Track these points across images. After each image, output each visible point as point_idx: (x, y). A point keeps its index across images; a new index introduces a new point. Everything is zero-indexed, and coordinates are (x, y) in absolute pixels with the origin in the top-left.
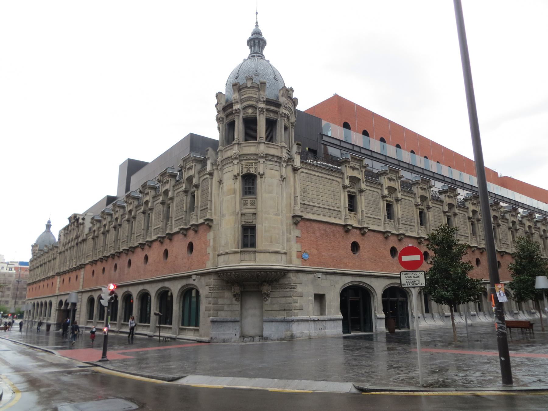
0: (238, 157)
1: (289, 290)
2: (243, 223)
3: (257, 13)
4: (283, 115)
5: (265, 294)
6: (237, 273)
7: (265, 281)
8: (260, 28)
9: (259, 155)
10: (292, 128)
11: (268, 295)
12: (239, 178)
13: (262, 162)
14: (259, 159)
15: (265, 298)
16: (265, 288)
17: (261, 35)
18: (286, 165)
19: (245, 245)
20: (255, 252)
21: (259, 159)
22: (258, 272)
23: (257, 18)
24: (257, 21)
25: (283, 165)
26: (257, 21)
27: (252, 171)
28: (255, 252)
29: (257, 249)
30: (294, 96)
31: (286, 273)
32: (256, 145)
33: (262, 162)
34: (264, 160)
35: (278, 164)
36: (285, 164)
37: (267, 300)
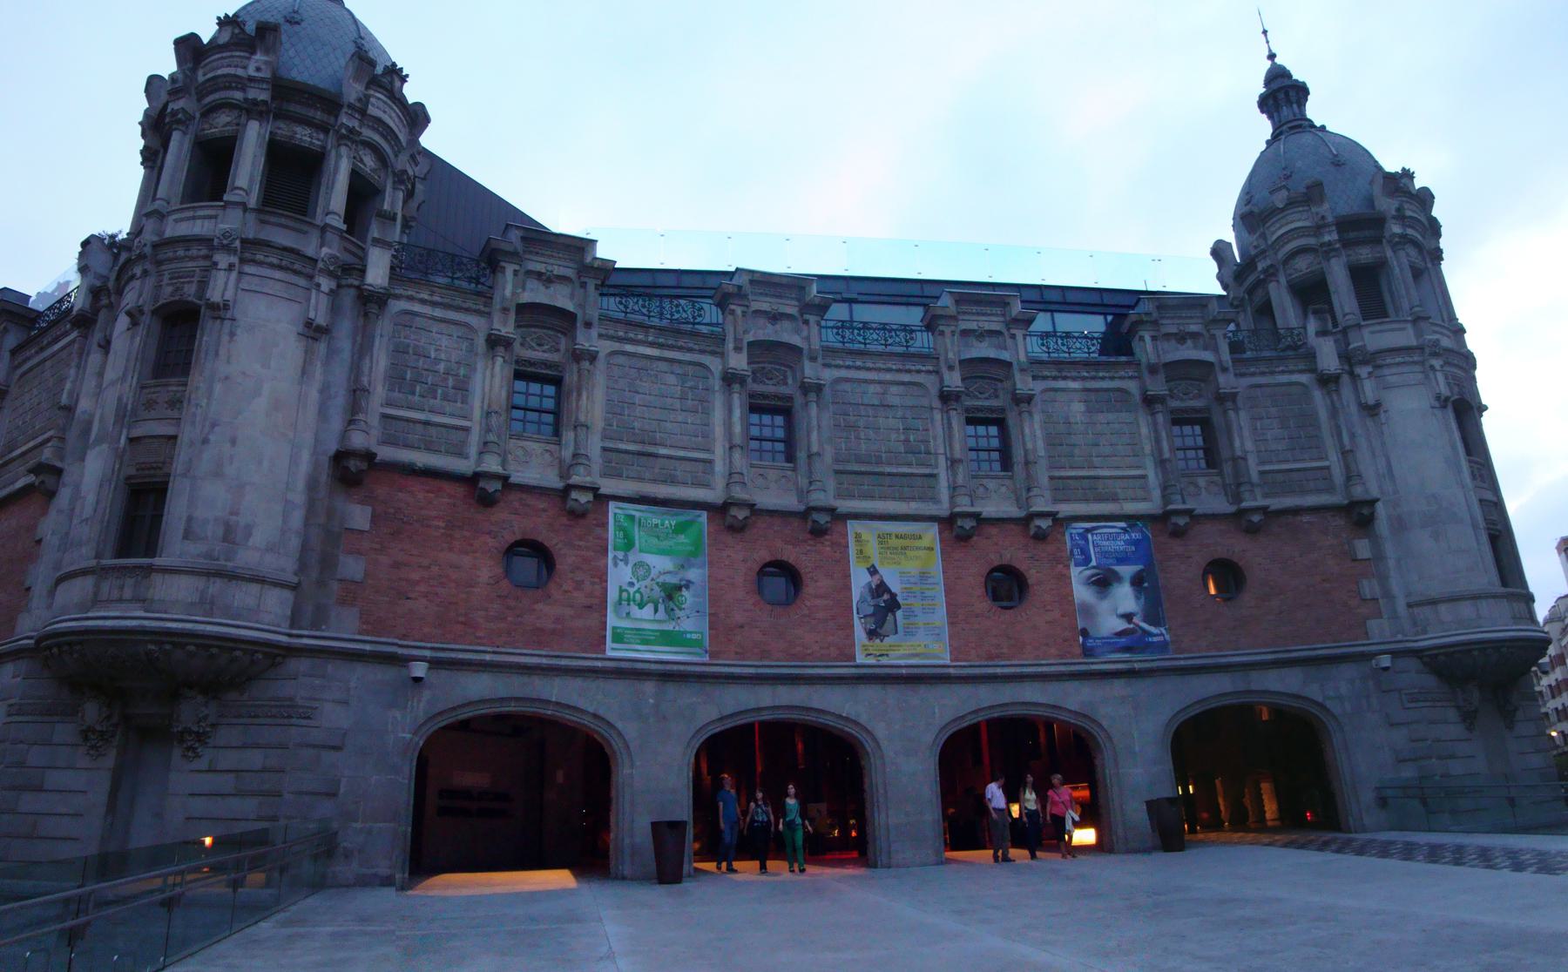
0: (148, 250)
1: (269, 721)
2: (132, 471)
4: (343, 131)
5: (190, 732)
6: (78, 647)
9: (216, 242)
10: (394, 189)
11: (201, 737)
12: (146, 319)
13: (223, 264)
14: (218, 257)
15: (188, 749)
16: (189, 712)
18: (333, 285)
19: (124, 549)
21: (218, 257)
22: (151, 642)
25: (318, 285)
27: (190, 290)
28: (150, 570)
29: (157, 561)
30: (411, 93)
31: (279, 659)
32: (220, 212)
33: (223, 264)
34: (234, 259)
35: (302, 282)
36: (326, 284)
37: (198, 756)
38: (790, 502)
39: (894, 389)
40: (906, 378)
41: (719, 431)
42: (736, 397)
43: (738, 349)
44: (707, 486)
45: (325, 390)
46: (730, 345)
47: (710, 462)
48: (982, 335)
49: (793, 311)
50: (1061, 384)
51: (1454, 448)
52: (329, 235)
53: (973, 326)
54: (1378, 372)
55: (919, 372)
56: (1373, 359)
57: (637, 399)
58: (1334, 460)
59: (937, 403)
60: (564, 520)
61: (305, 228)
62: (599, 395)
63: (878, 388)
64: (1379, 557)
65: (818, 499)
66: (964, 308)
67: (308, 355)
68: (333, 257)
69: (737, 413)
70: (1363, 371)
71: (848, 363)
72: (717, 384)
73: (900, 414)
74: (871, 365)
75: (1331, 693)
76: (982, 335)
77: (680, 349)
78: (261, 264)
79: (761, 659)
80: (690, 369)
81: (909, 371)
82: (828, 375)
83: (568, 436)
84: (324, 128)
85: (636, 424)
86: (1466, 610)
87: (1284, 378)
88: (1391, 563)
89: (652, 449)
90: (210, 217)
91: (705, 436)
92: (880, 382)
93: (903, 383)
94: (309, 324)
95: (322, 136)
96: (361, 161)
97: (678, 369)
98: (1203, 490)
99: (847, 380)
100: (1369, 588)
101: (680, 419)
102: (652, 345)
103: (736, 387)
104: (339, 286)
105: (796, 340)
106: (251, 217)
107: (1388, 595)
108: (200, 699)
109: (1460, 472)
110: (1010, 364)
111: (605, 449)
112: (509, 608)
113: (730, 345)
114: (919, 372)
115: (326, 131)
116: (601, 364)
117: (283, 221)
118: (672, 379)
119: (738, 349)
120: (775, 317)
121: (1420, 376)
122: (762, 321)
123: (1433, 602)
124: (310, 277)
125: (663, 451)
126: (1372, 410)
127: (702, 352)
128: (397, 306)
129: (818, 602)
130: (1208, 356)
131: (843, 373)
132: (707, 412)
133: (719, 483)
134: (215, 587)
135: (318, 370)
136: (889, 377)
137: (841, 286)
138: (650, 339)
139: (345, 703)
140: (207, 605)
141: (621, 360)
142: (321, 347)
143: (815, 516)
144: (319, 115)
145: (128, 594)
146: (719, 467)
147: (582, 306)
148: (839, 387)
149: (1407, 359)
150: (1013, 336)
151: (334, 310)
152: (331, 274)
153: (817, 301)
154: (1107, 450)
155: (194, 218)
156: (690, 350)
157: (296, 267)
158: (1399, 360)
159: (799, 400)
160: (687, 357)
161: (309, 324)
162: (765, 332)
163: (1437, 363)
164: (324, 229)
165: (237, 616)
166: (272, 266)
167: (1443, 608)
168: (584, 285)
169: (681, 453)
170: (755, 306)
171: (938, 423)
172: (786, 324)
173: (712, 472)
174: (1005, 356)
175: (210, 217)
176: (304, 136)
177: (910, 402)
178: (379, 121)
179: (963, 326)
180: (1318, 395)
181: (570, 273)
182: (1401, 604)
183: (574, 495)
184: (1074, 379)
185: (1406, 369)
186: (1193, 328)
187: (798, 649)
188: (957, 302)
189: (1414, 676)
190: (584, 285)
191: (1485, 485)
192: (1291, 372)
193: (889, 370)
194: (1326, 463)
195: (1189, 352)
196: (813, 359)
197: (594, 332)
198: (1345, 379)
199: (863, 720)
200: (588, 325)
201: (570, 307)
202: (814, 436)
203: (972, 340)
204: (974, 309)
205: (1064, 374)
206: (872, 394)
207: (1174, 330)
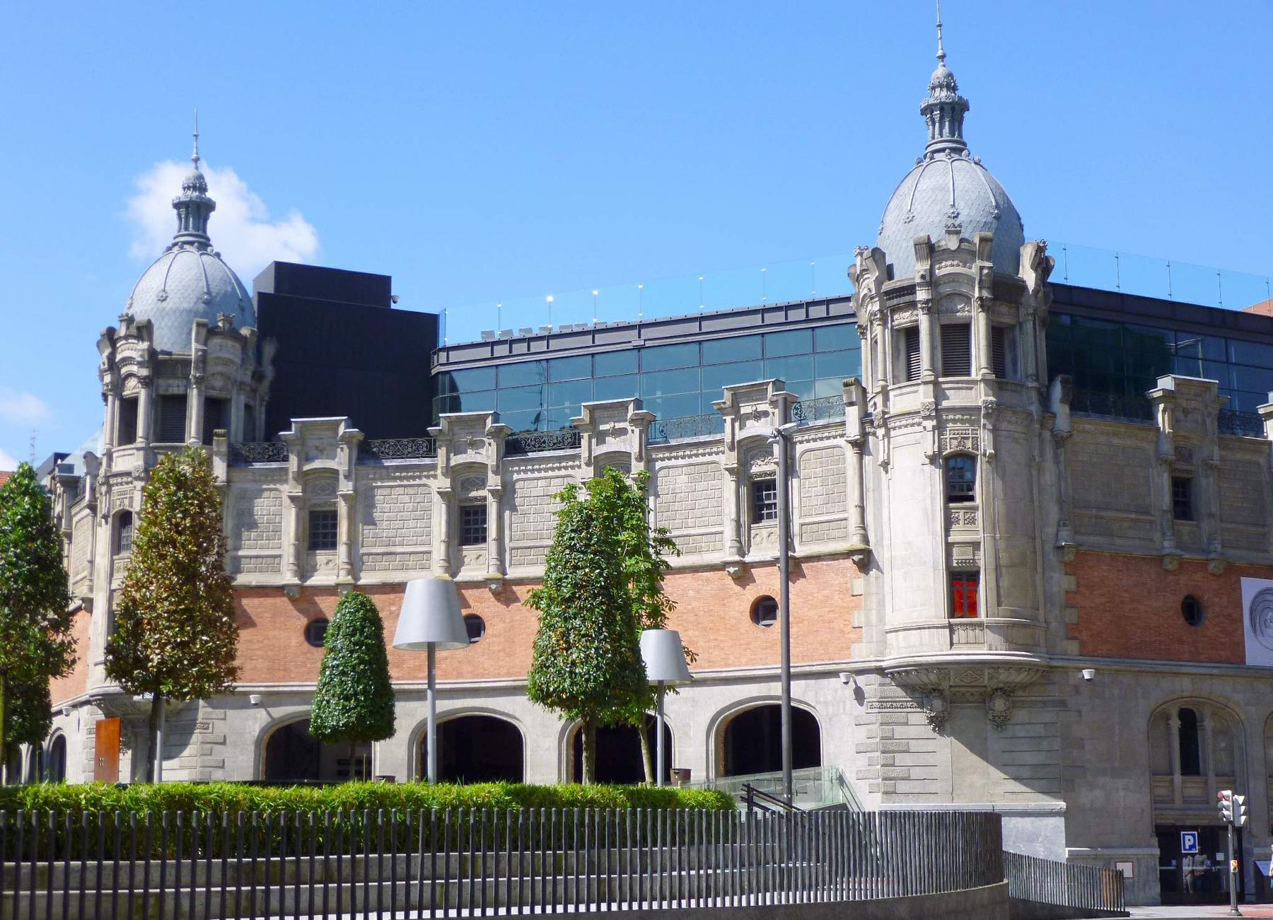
12: (110, 520)
50: (673, 462)
79: (457, 678)
90: (131, 455)
92: (545, 478)
97: (411, 491)
100: (857, 618)
109: (933, 520)
112: (309, 659)
118: (406, 498)
125: (399, 549)
128: (236, 486)
129: (495, 639)
136: (550, 473)
154: (698, 512)
155: (124, 455)
158: (904, 422)
175: (131, 455)
185: (910, 429)
187: (482, 670)
194: (845, 515)
199: (517, 715)
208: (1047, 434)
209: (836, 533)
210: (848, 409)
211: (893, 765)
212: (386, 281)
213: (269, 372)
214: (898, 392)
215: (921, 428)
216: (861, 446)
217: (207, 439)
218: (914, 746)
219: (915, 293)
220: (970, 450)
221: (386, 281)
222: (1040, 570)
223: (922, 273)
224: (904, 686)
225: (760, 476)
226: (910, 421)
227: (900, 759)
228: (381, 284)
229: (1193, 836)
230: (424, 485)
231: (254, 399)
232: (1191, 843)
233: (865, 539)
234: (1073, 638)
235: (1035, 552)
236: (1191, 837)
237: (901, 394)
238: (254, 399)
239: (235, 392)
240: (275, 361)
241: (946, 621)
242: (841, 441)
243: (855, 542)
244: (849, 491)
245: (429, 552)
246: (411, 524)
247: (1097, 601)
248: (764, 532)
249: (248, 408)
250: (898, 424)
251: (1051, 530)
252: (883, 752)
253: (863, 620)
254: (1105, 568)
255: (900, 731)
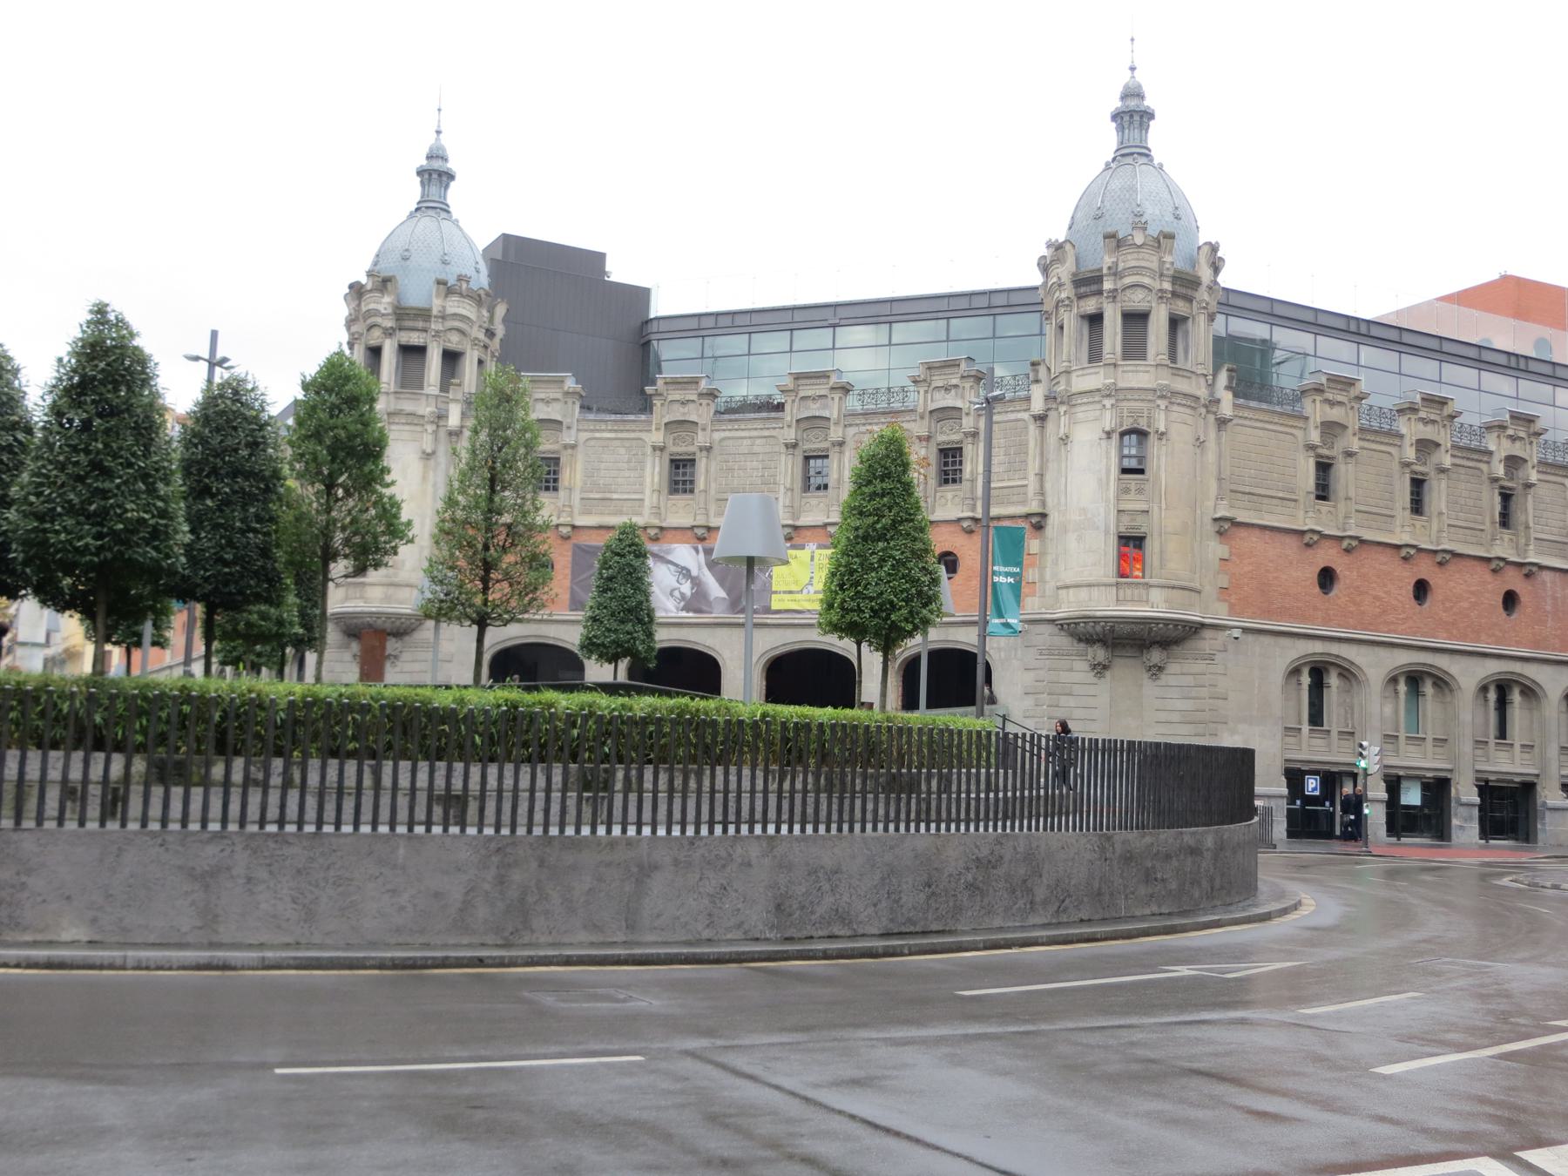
3: (439, 110)
7: (389, 634)
8: (445, 140)
11: (396, 657)
17: (445, 159)
18: (434, 427)
20: (363, 584)
23: (439, 121)
24: (439, 126)
26: (439, 126)
28: (363, 584)
35: (419, 428)
36: (430, 428)
38: (687, 521)
39: (758, 441)
40: (766, 433)
41: (648, 480)
42: (657, 459)
43: (657, 429)
44: (640, 514)
45: (435, 485)
46: (654, 427)
47: (642, 500)
48: (814, 399)
49: (694, 397)
51: (1108, 471)
52: (430, 399)
53: (809, 393)
54: (1074, 410)
55: (775, 428)
56: (1069, 399)
57: (603, 466)
58: (1032, 483)
59: (783, 449)
60: (559, 542)
61: (418, 397)
62: (579, 466)
63: (749, 442)
64: (1043, 553)
65: (701, 521)
66: (801, 382)
67: (425, 467)
68: (434, 412)
69: (657, 469)
70: (1063, 409)
71: (730, 427)
72: (649, 450)
73: (761, 457)
74: (743, 427)
75: (995, 645)
76: (814, 399)
77: (628, 431)
78: (397, 423)
80: (634, 443)
81: (768, 429)
82: (717, 436)
83: (562, 493)
84: (425, 330)
85: (601, 482)
86: (1084, 593)
87: (1012, 416)
88: (1049, 558)
89: (608, 495)
91: (641, 484)
92: (750, 438)
93: (765, 437)
94: (424, 452)
95: (424, 334)
96: (449, 341)
97: (627, 444)
98: (949, 503)
99: (729, 438)
101: (627, 475)
102: (610, 431)
103: (658, 453)
104: (438, 426)
105: (693, 418)
106: (392, 397)
107: (1042, 580)
108: (394, 640)
109: (1108, 489)
110: (828, 419)
111: (582, 499)
113: (654, 427)
114: (775, 428)
115: (426, 331)
116: (580, 448)
117: (408, 396)
118: (622, 451)
119: (657, 429)
120: (684, 403)
121: (1098, 413)
122: (676, 406)
123: (1067, 587)
124: (423, 425)
125: (615, 496)
126: (1065, 440)
127: (640, 431)
130: (959, 404)
131: (727, 434)
132: (643, 469)
133: (646, 511)
134: (391, 590)
135: (431, 475)
137: (828, 313)
138: (609, 428)
139: (452, 640)
140: (387, 599)
141: (592, 443)
142: (432, 462)
143: (696, 530)
144: (420, 324)
145: (358, 595)
146: (647, 503)
147: (565, 416)
148: (724, 443)
149: (1091, 400)
150: (833, 399)
151: (436, 440)
152: (432, 422)
153: (705, 391)
156: (634, 431)
157: (416, 422)
158: (1085, 400)
159: (698, 454)
160: (632, 435)
161: (424, 452)
162: (678, 413)
163: (1108, 402)
164: (427, 395)
165: (401, 603)
166: (403, 424)
167: (1071, 591)
168: (566, 403)
169: (626, 496)
170: (670, 398)
171: (783, 463)
172: (691, 406)
173: (641, 506)
174: (826, 414)
176: (415, 339)
177: (768, 449)
178: (455, 314)
179: (802, 394)
180: (1033, 428)
181: (559, 396)
182: (1051, 585)
183: (561, 529)
184: (877, 424)
186: (954, 382)
188: (796, 379)
189: (1045, 635)
190: (566, 403)
191: (1142, 497)
192: (1019, 411)
193: (756, 429)
194: (1025, 482)
195: (949, 400)
196: (704, 430)
197: (573, 431)
198: (1052, 414)
199: (717, 648)
200: (569, 428)
201: (559, 418)
202: (702, 479)
203: (810, 403)
204: (808, 381)
205: (869, 421)
206: (745, 446)
207: (940, 384)
208: (1211, 418)
209: (1015, 498)
210: (1034, 387)
211: (1057, 706)
212: (601, 257)
213: (500, 331)
214: (1080, 372)
215: (1099, 406)
216: (1041, 419)
217: (445, 386)
218: (1077, 689)
219: (1102, 282)
220: (1145, 428)
221: (601, 257)
222: (1198, 539)
223: (1110, 264)
224: (1072, 635)
225: (948, 443)
226: (1091, 400)
227: (1063, 700)
228: (598, 259)
229: (1316, 779)
230: (640, 439)
231: (486, 355)
232: (1314, 785)
233: (1043, 503)
234: (1225, 600)
235: (1195, 523)
236: (1314, 782)
237: (1083, 375)
238: (486, 355)
239: (469, 347)
240: (505, 320)
241: (1114, 580)
242: (1025, 416)
243: (1034, 507)
244: (1030, 462)
245: (642, 500)
246: (627, 474)
247: (1246, 569)
248: (949, 495)
249: (480, 362)
250: (1079, 401)
251: (1210, 504)
252: (1049, 694)
253: (1037, 576)
254: (1255, 539)
255: (1065, 677)
